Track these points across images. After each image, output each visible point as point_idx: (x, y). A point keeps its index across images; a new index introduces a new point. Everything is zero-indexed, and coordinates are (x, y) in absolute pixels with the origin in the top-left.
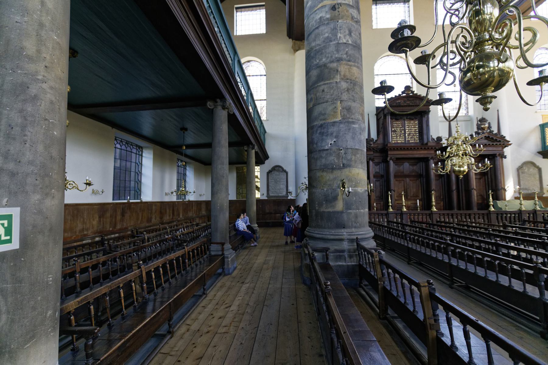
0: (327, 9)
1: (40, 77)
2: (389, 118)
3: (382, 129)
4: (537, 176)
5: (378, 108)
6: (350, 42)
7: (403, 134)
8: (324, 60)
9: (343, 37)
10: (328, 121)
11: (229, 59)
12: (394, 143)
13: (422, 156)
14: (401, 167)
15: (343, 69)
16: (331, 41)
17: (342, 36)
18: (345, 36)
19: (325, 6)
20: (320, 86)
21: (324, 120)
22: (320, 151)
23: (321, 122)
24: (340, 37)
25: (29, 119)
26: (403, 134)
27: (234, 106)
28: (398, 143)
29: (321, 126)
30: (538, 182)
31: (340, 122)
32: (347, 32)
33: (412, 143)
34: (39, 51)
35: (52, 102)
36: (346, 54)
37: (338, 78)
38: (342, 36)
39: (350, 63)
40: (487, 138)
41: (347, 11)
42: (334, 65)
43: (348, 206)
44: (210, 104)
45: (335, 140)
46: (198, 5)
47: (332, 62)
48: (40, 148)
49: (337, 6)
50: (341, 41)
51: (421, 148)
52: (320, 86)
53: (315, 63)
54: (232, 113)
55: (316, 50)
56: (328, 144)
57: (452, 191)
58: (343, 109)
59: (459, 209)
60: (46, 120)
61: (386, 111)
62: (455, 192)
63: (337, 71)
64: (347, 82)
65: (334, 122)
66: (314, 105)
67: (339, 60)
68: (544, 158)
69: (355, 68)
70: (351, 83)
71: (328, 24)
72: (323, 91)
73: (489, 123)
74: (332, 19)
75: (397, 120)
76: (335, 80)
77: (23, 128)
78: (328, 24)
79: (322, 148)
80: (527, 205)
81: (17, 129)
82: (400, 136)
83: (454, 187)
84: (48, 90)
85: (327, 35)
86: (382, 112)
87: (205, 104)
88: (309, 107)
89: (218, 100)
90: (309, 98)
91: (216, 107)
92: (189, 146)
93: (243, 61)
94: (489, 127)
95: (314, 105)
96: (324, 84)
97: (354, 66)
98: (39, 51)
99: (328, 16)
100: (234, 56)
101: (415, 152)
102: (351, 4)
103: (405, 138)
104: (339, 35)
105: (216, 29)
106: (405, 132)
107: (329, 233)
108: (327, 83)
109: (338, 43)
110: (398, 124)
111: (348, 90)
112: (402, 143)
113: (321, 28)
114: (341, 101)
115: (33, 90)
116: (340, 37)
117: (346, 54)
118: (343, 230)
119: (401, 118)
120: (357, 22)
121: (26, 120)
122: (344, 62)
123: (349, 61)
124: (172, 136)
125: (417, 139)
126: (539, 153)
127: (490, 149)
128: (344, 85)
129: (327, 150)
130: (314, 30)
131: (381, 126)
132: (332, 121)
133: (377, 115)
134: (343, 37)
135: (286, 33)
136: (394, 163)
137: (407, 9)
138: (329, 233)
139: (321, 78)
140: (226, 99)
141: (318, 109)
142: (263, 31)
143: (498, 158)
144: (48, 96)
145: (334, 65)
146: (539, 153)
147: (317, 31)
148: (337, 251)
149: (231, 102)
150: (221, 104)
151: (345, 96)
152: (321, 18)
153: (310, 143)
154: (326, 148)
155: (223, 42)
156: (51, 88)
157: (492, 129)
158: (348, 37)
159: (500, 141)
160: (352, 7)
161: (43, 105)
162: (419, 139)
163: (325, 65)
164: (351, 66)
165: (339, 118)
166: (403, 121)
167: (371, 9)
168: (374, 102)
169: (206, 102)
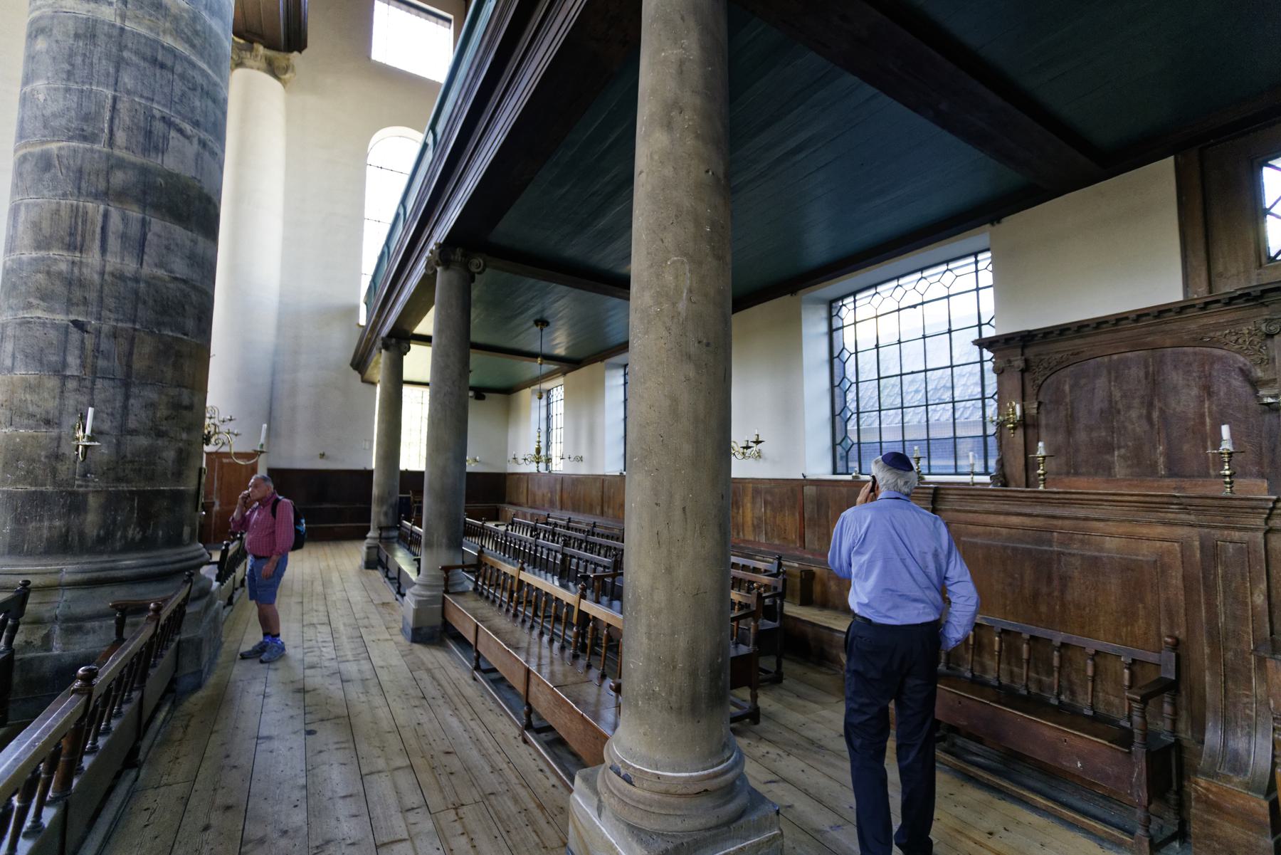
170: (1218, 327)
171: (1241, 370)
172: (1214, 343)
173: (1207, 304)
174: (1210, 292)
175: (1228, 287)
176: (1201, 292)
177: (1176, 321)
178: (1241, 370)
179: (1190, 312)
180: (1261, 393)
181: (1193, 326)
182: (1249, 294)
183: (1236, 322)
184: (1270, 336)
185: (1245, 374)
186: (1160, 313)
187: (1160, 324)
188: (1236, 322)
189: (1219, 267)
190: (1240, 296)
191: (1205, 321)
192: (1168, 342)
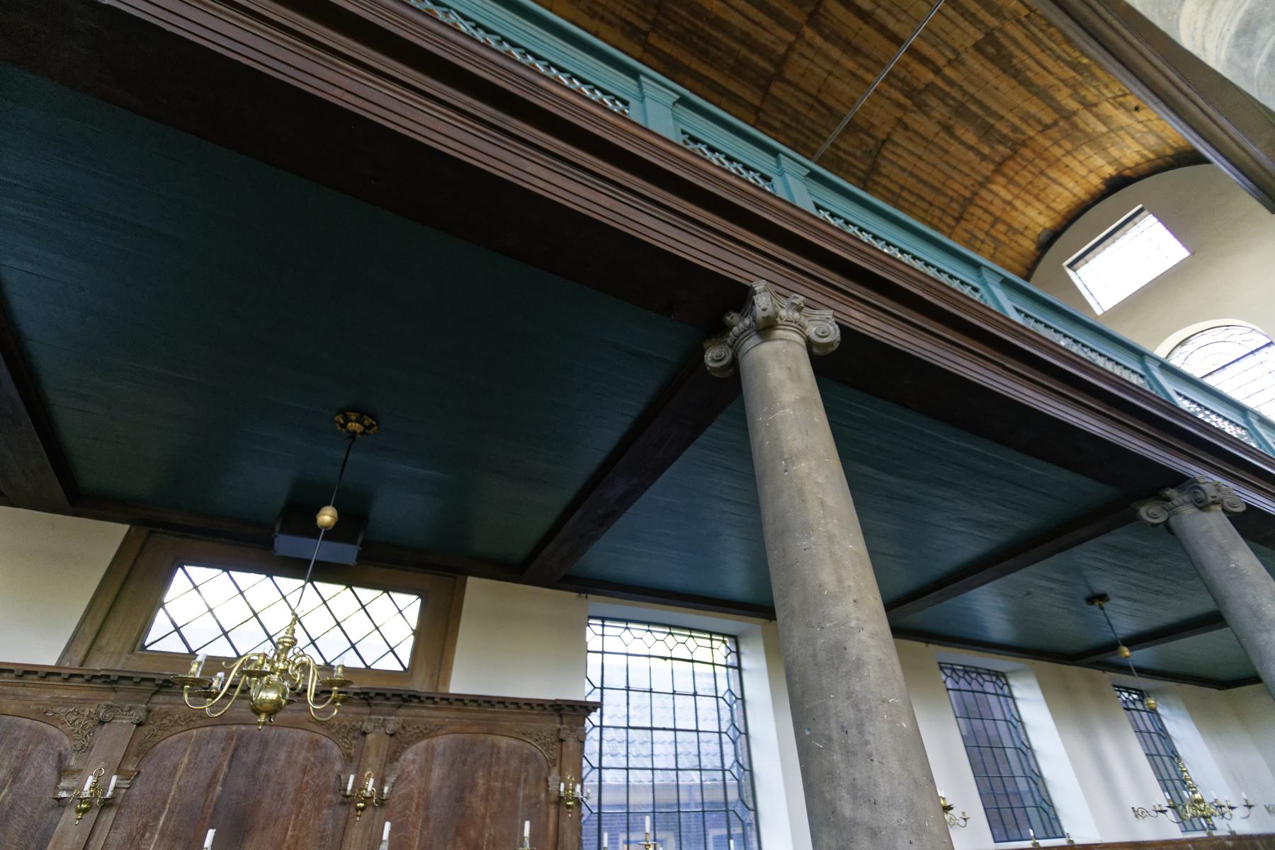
1: (853, 624)
11: (1135, 380)
25: (863, 707)
27: (1231, 485)
34: (840, 580)
35: (881, 664)
44: (1150, 513)
46: (1016, 337)
48: (894, 765)
54: (1242, 509)
60: (884, 701)
77: (860, 726)
81: (853, 732)
84: (871, 642)
87: (1135, 517)
89: (1171, 492)
91: (1172, 512)
92: (1135, 641)
93: (1161, 352)
98: (840, 580)
100: (1142, 363)
105: (1063, 343)
115: (853, 652)
121: (860, 711)
124: (1071, 626)
140: (1195, 480)
142: (1184, 253)
144: (873, 652)
149: (1217, 479)
150: (1186, 498)
155: (1093, 355)
156: (872, 636)
161: (872, 672)
169: (1136, 512)
170: (66, 702)
171: (60, 755)
172: (54, 721)
173: (72, 676)
174: (82, 665)
175: (99, 664)
176: (73, 664)
177: (35, 685)
178: (60, 755)
179: (53, 681)
180: (64, 784)
181: (46, 696)
182: (109, 676)
183: (85, 701)
184: (102, 722)
185: (61, 759)
186: (27, 672)
187: (17, 685)
188: (85, 701)
189: (103, 642)
190: (102, 676)
191: (58, 693)
192: (13, 708)
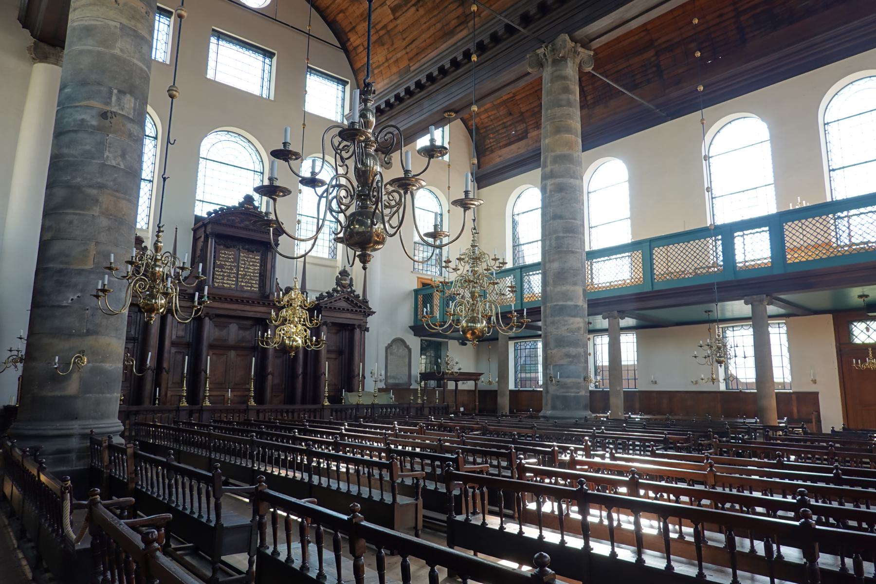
0: (94, 112)
2: (211, 242)
3: (198, 256)
4: (407, 360)
5: (198, 219)
6: (122, 167)
7: (236, 272)
8: (79, 180)
9: (111, 158)
10: (72, 267)
12: (217, 288)
13: (259, 315)
14: (224, 333)
15: (106, 199)
16: (94, 158)
17: (110, 155)
18: (115, 158)
19: (92, 108)
20: (67, 214)
21: (67, 263)
22: (53, 306)
23: (61, 266)
24: (108, 157)
26: (236, 272)
28: (224, 288)
29: (60, 271)
30: (407, 368)
31: (91, 271)
32: (119, 153)
33: (247, 291)
36: (114, 181)
37: (96, 211)
38: (110, 155)
39: (117, 194)
40: (347, 300)
41: (124, 125)
42: (93, 192)
43: (86, 387)
45: (79, 294)
47: (90, 186)
49: (109, 115)
50: (109, 163)
51: (259, 303)
52: (67, 214)
53: (65, 178)
55: (68, 161)
56: (68, 299)
57: (298, 376)
58: (98, 253)
59: (303, 402)
61: (209, 230)
62: (301, 377)
63: (97, 201)
64: (110, 219)
65: (83, 270)
66: (53, 239)
67: (101, 187)
68: (415, 335)
69: (124, 202)
70: (116, 220)
71: (92, 132)
72: (71, 222)
73: (351, 279)
74: (99, 129)
75: (227, 247)
76: (92, 213)
78: (92, 132)
79: (57, 303)
80: (383, 400)
82: (229, 276)
83: (300, 371)
85: (88, 147)
86: (203, 229)
88: (45, 238)
90: (47, 224)
94: (351, 285)
95: (53, 239)
96: (74, 214)
97: (124, 199)
99: (94, 123)
101: (248, 308)
102: (131, 116)
103: (237, 281)
104: (107, 154)
106: (238, 271)
107: (49, 428)
108: (80, 214)
109: (104, 165)
110: (227, 255)
111: (109, 229)
112: (230, 289)
113: (81, 135)
114: (97, 243)
116: (108, 157)
117: (114, 181)
118: (74, 422)
119: (234, 246)
120: (136, 141)
122: (109, 191)
123: (117, 191)
125: (256, 288)
126: (411, 327)
127: (349, 316)
128: (104, 222)
129: (65, 307)
130: (69, 131)
131: (198, 252)
132: (79, 267)
133: (195, 230)
134: (111, 158)
135: (16, 14)
136: (210, 319)
137: (267, 67)
138: (49, 428)
139: (69, 203)
141: (57, 248)
143: (357, 331)
145: (93, 192)
146: (411, 327)
147: (73, 135)
148: (59, 452)
151: (103, 237)
152: (83, 120)
153: (38, 292)
154: (65, 303)
157: (354, 288)
158: (119, 159)
159: (360, 307)
160: (132, 121)
162: (260, 287)
163: (79, 188)
164: (118, 198)
165: (90, 266)
166: (237, 252)
167: (209, 42)
168: (193, 206)
